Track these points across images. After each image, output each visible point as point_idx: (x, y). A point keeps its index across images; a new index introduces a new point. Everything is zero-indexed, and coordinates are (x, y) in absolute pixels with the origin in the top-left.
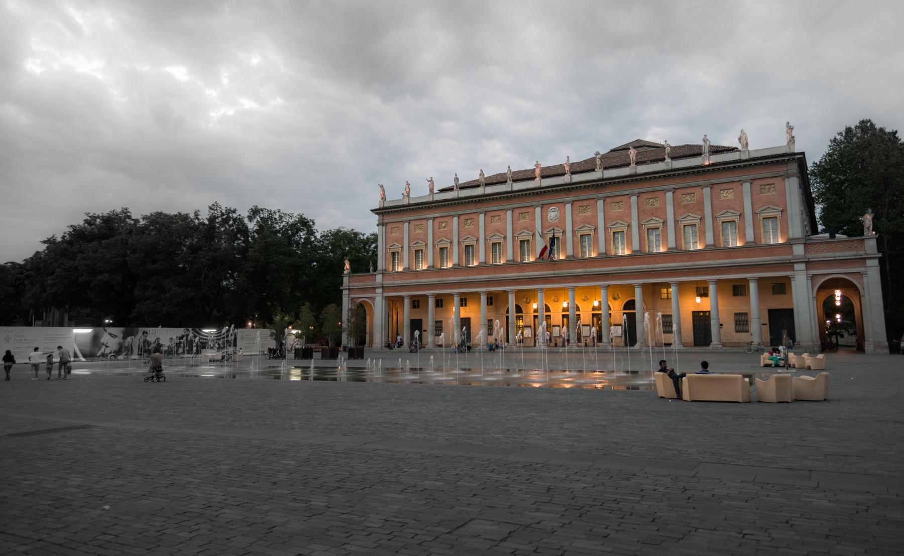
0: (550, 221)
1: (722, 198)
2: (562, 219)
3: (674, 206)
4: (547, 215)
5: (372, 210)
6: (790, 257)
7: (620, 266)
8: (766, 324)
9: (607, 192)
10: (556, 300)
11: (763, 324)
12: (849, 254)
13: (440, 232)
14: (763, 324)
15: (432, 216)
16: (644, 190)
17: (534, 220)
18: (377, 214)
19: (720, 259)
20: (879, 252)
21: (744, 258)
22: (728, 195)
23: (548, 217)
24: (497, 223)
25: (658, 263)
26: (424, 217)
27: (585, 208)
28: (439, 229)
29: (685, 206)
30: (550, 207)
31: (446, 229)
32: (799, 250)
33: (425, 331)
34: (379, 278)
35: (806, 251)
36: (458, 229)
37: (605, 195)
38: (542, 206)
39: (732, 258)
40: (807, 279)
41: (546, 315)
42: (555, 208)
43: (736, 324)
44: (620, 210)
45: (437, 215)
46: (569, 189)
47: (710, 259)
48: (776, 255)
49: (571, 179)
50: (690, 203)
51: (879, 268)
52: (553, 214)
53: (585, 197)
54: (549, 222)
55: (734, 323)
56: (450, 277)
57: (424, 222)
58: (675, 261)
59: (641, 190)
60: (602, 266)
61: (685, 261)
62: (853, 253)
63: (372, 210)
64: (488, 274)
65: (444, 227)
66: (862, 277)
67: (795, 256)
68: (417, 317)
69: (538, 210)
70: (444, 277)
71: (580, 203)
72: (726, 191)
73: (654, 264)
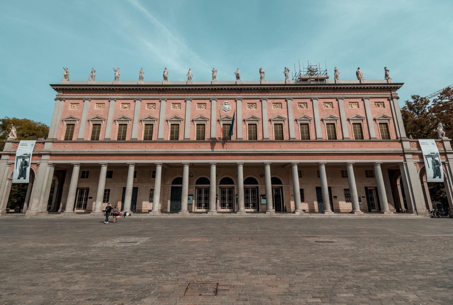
3: (319, 110)
5: (52, 85)
7: (282, 148)
8: (364, 197)
9: (270, 95)
11: (363, 197)
13: (121, 111)
14: (363, 197)
18: (56, 90)
19: (355, 148)
21: (371, 148)
25: (310, 148)
27: (251, 105)
31: (128, 109)
33: (91, 198)
34: (48, 147)
37: (268, 97)
42: (228, 102)
43: (346, 197)
44: (278, 109)
46: (241, 89)
47: (348, 147)
55: (344, 196)
56: (126, 149)
57: (106, 102)
58: (323, 148)
60: (267, 148)
61: (330, 148)
63: (52, 85)
67: (405, 149)
68: (84, 185)
70: (120, 148)
73: (307, 148)
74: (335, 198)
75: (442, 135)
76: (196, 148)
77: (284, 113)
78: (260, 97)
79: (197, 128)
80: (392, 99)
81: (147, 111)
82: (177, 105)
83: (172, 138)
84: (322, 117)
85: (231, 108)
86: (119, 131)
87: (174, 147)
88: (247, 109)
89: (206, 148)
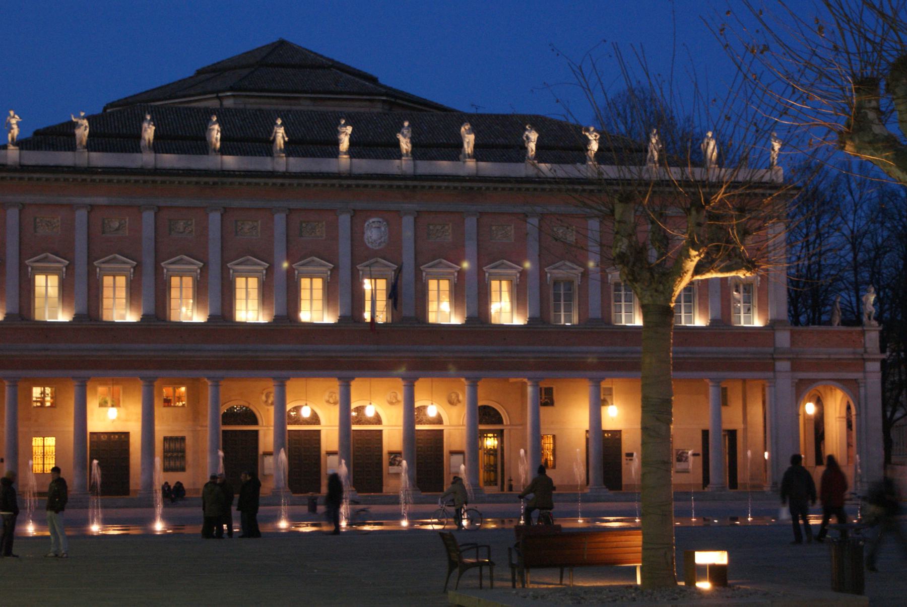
0: (370, 245)
4: (363, 233)
10: (331, 401)
12: (845, 352)
15: (88, 200)
20: (883, 350)
23: (366, 236)
26: (64, 200)
28: (103, 232)
30: (371, 217)
32: (783, 338)
35: (793, 342)
36: (156, 238)
38: (355, 214)
40: (792, 386)
41: (223, 431)
45: (102, 200)
49: (415, 166)
51: (880, 375)
54: (368, 248)
62: (851, 350)
65: (117, 229)
66: (859, 387)
69: (344, 220)
74: (628, 458)
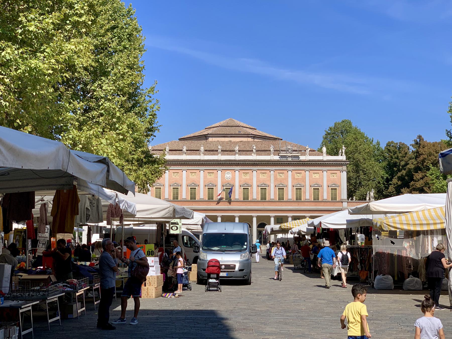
0: (227, 179)
1: (313, 177)
2: (234, 178)
3: (292, 178)
6: (342, 207)
9: (259, 168)
16: (278, 169)
17: (217, 177)
22: (317, 176)
24: (193, 177)
29: (297, 179)
32: (345, 204)
37: (257, 169)
39: (317, 206)
44: (264, 177)
48: (335, 206)
50: (299, 177)
52: (228, 175)
53: (247, 168)
59: (276, 169)
60: (255, 206)
64: (188, 205)
71: (244, 171)
72: (315, 174)
75: (372, 197)
76: (208, 206)
77: (268, 181)
78: (252, 169)
79: (208, 191)
80: (342, 172)
81: (174, 178)
82: (194, 174)
83: (191, 198)
84: (293, 184)
85: (231, 177)
86: (156, 192)
87: (194, 204)
88: (243, 177)
89: (214, 206)
